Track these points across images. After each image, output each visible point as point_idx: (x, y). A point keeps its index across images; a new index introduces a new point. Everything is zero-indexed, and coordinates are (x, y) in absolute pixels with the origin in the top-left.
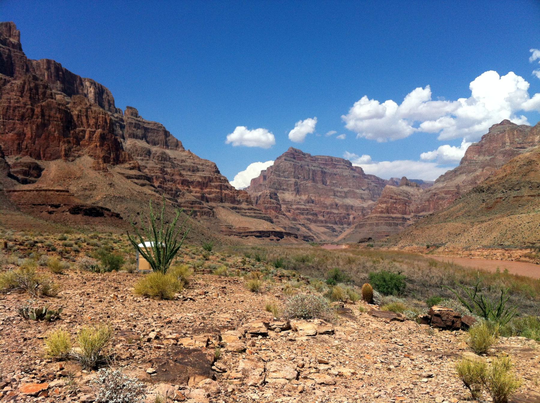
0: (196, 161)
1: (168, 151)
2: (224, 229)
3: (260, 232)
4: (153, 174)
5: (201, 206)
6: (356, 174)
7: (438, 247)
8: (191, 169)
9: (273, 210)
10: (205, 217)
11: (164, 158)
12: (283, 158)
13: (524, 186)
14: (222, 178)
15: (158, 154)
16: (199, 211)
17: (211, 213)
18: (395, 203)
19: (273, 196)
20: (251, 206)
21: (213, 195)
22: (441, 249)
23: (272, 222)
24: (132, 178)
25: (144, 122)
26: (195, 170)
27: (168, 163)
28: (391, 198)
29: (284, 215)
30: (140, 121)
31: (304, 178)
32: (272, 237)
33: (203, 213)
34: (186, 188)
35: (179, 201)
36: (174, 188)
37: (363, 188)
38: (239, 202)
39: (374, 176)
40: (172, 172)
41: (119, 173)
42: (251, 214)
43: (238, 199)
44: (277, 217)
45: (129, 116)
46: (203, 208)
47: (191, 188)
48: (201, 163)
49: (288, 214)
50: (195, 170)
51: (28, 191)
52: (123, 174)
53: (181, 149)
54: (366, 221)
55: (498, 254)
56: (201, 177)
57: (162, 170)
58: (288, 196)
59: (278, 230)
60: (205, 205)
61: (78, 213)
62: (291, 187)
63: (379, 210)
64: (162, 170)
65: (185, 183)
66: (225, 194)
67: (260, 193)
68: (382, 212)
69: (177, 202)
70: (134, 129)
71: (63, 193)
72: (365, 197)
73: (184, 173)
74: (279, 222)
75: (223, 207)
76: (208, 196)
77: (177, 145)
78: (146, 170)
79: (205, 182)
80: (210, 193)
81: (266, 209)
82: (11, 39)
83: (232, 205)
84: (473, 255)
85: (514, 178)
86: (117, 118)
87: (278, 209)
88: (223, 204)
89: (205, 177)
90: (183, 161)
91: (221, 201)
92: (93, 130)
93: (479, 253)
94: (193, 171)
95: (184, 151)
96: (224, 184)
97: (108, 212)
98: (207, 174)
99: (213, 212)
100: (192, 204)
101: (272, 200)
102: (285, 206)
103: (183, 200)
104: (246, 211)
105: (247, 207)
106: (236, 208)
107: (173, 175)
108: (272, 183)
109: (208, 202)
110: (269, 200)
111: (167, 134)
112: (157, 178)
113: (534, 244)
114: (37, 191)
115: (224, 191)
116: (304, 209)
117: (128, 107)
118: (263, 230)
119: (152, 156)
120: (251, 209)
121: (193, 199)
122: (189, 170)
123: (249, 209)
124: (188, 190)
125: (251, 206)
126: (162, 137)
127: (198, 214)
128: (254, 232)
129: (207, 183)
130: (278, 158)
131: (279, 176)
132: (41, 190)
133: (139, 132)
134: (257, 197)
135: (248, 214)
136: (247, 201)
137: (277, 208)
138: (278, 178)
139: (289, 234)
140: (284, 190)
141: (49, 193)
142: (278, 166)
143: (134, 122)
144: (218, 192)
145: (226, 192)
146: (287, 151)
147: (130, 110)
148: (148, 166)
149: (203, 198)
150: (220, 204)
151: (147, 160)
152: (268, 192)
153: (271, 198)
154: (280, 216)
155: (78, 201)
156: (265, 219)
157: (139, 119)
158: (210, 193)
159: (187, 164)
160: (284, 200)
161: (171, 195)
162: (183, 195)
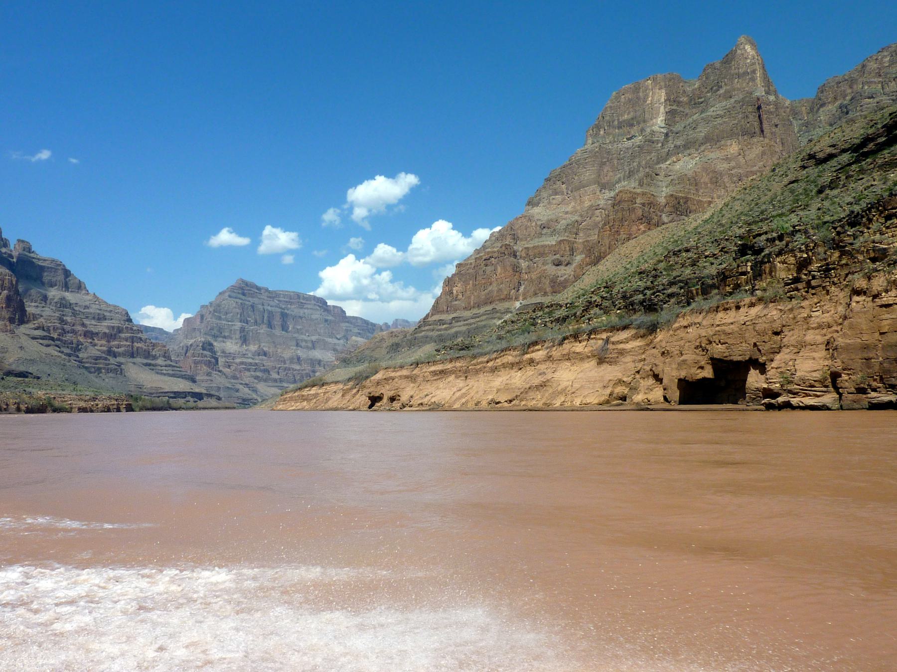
0: (103, 307)
1: (70, 296)
2: (132, 389)
3: (175, 393)
9: (205, 365)
10: (111, 375)
11: (63, 304)
14: (135, 328)
16: (104, 368)
17: (118, 370)
19: (208, 346)
20: (169, 362)
23: (194, 381)
26: (101, 318)
27: (68, 311)
29: (220, 371)
31: (256, 321)
32: (189, 398)
33: (108, 371)
34: (90, 341)
35: (81, 355)
36: (75, 341)
38: (155, 357)
43: (154, 353)
44: (209, 374)
47: (96, 341)
49: (226, 370)
50: (101, 318)
56: (108, 327)
57: (62, 321)
58: (231, 346)
59: (197, 390)
60: (112, 360)
62: (235, 334)
64: (62, 321)
65: (89, 334)
66: (138, 348)
69: (78, 357)
73: (87, 322)
75: (134, 363)
76: (116, 350)
78: (41, 320)
79: (113, 333)
80: (118, 347)
81: (196, 363)
83: (145, 361)
85: (367, 352)
87: (213, 363)
88: (135, 360)
89: (113, 327)
90: (86, 307)
91: (132, 356)
94: (99, 319)
98: (115, 323)
101: (205, 352)
102: (223, 360)
106: (150, 365)
109: (115, 357)
110: (201, 351)
112: (55, 329)
115: (135, 344)
116: (251, 364)
119: (48, 302)
120: (170, 366)
121: (98, 354)
122: (94, 318)
125: (169, 362)
129: (115, 335)
136: (164, 357)
139: (210, 396)
140: (225, 337)
145: (139, 345)
148: (44, 314)
149: (110, 352)
150: (131, 360)
152: (201, 339)
153: (204, 349)
156: (186, 379)
158: (118, 347)
159: (91, 310)
160: (223, 352)
161: (72, 348)
162: (86, 349)
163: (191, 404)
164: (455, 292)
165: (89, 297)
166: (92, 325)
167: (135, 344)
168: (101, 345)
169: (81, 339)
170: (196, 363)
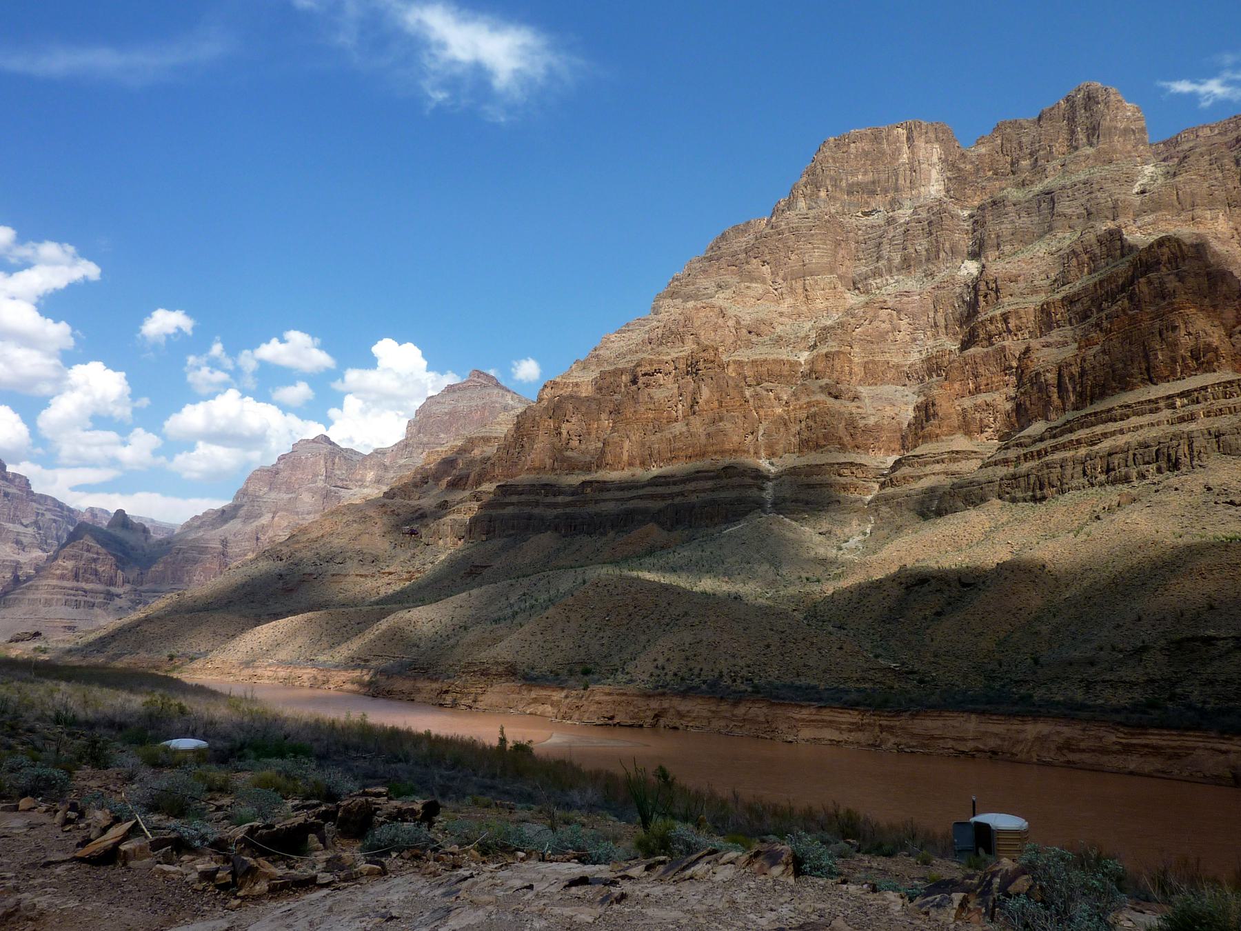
6: (12, 490)
7: (192, 659)
13: (350, 558)
18: (95, 560)
22: (197, 664)
28: (88, 551)
37: (25, 522)
39: (54, 499)
54: (23, 593)
55: (305, 677)
63: (58, 572)
68: (62, 577)
72: (25, 540)
84: (260, 677)
93: (270, 673)
113: (367, 661)
164: (564, 432)
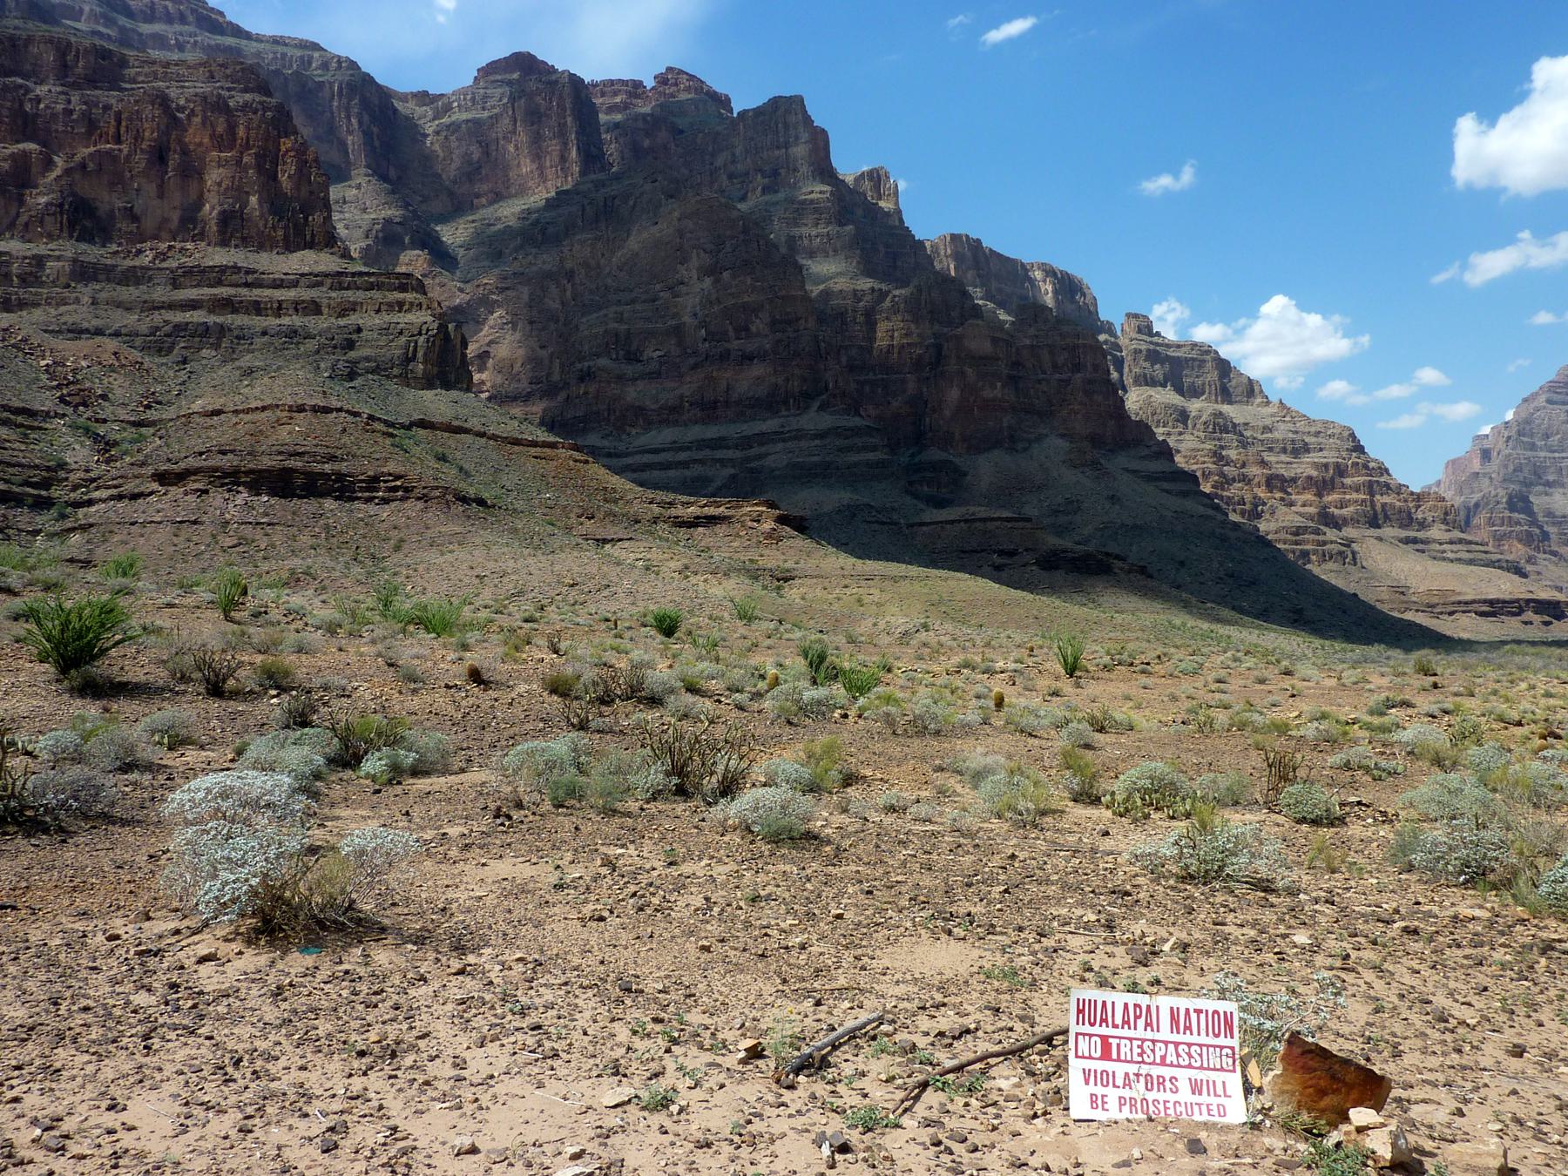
0: (1301, 426)
2: (1385, 596)
3: (1491, 602)
4: (1194, 467)
5: (1321, 538)
8: (1289, 448)
9: (1520, 541)
10: (1331, 565)
11: (1221, 426)
12: (1543, 398)
15: (1204, 419)
16: (1315, 552)
17: (1347, 555)
19: (1519, 503)
20: (1456, 534)
21: (1351, 509)
23: (1524, 575)
24: (1157, 479)
25: (1168, 346)
29: (1554, 554)
30: (1157, 344)
32: (1529, 615)
33: (1325, 557)
34: (1278, 495)
35: (1263, 526)
36: (1248, 497)
38: (1423, 525)
40: (1243, 458)
41: (1126, 470)
42: (1458, 555)
43: (1420, 516)
44: (1530, 560)
45: (1134, 335)
46: (1324, 543)
48: (1313, 430)
51: (947, 522)
52: (1134, 472)
53: (1259, 400)
56: (1316, 465)
57: (1218, 456)
59: (1544, 595)
60: (1331, 534)
61: (1057, 568)
64: (1218, 456)
65: (1274, 482)
66: (1384, 505)
67: (1476, 497)
70: (1147, 365)
71: (1021, 524)
74: (1539, 573)
75: (1380, 539)
76: (1336, 512)
77: (1251, 389)
82: (882, 204)
83: (1404, 533)
86: (1106, 342)
88: (1377, 532)
89: (1326, 466)
91: (1374, 523)
92: (1063, 376)
95: (1268, 403)
96: (1377, 478)
97: (1120, 564)
98: (1330, 457)
99: (1354, 553)
100: (1296, 534)
103: (1272, 526)
104: (1445, 547)
105: (1447, 536)
106: (1415, 541)
107: (1243, 466)
108: (1511, 468)
110: (1507, 513)
111: (1224, 367)
112: (1206, 476)
114: (966, 521)
115: (1378, 497)
117: (1128, 315)
118: (1501, 596)
120: (1461, 541)
121: (1299, 521)
122: (1284, 451)
123: (1451, 542)
124: (1282, 499)
125: (1456, 534)
126: (1212, 376)
127: (1314, 558)
128: (1473, 602)
129: (1332, 479)
130: (1525, 400)
131: (1533, 447)
132: (975, 520)
133: (1159, 371)
134: (1468, 509)
135: (1450, 555)
136: (1445, 522)
137: (1529, 534)
138: (1529, 453)
140: (1548, 484)
141: (990, 526)
142: (1528, 421)
143: (1144, 347)
144: (1364, 501)
145: (1386, 499)
146: (1552, 376)
147: (1134, 323)
148: (1182, 447)
151: (1180, 434)
153: (1511, 511)
154: (1542, 556)
155: (1053, 541)
157: (1155, 339)
159: (1277, 435)
161: (1243, 513)
163: (1535, 633)
165: (1270, 410)
166: (1280, 464)
167: (1378, 497)
168: (1306, 501)
169: (1262, 493)
170: (1499, 539)
